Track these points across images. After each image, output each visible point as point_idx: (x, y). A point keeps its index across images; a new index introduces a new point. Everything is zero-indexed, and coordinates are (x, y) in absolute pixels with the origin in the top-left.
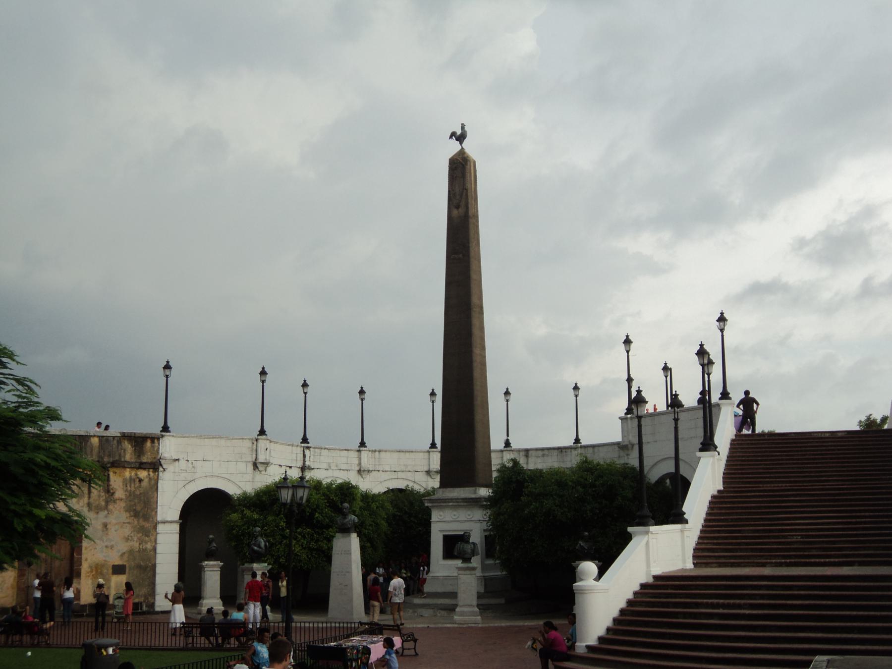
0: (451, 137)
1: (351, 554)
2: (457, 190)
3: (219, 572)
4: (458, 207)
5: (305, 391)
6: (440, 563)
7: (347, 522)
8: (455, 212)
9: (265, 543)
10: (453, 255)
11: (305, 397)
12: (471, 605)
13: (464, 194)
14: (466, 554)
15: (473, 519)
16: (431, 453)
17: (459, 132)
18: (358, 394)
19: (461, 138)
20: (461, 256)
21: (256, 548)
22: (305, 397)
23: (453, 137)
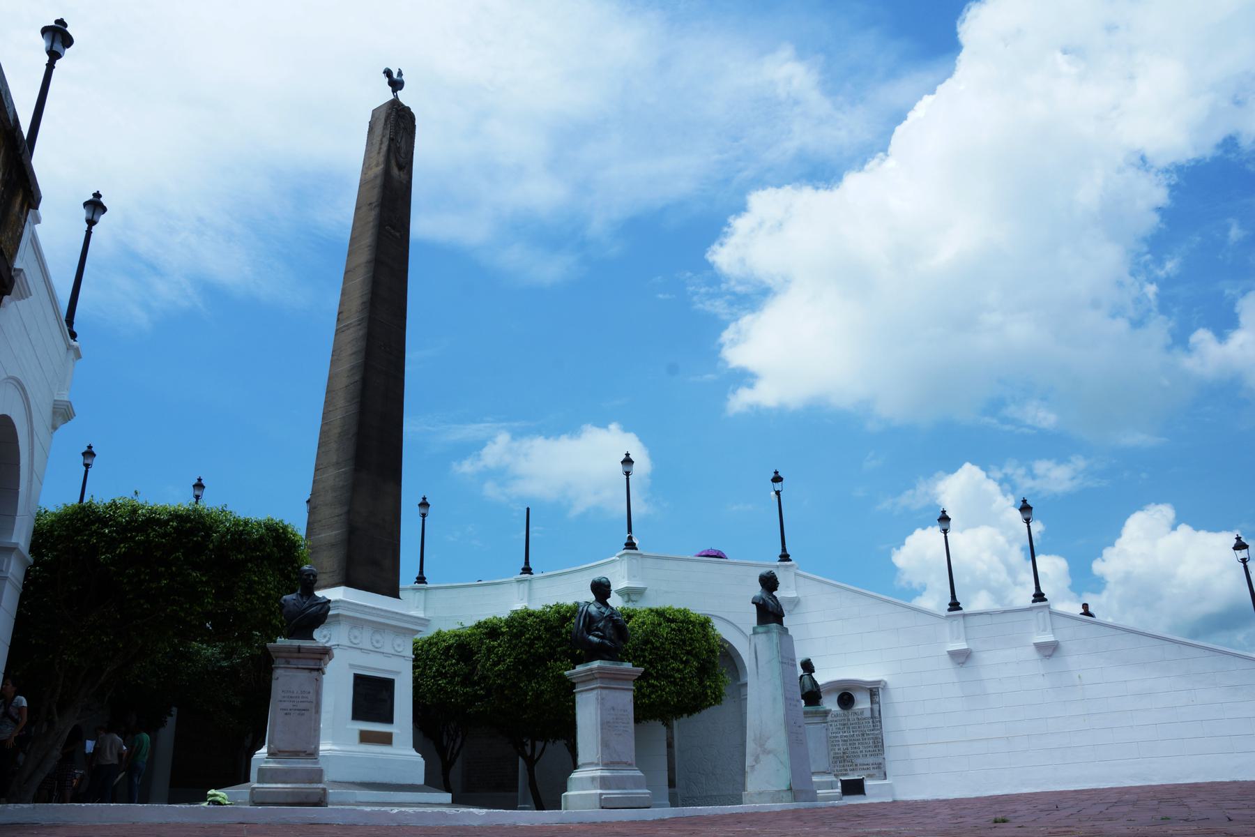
4: (400, 168)
6: (348, 727)
8: (395, 171)
19: (396, 84)
20: (398, 234)
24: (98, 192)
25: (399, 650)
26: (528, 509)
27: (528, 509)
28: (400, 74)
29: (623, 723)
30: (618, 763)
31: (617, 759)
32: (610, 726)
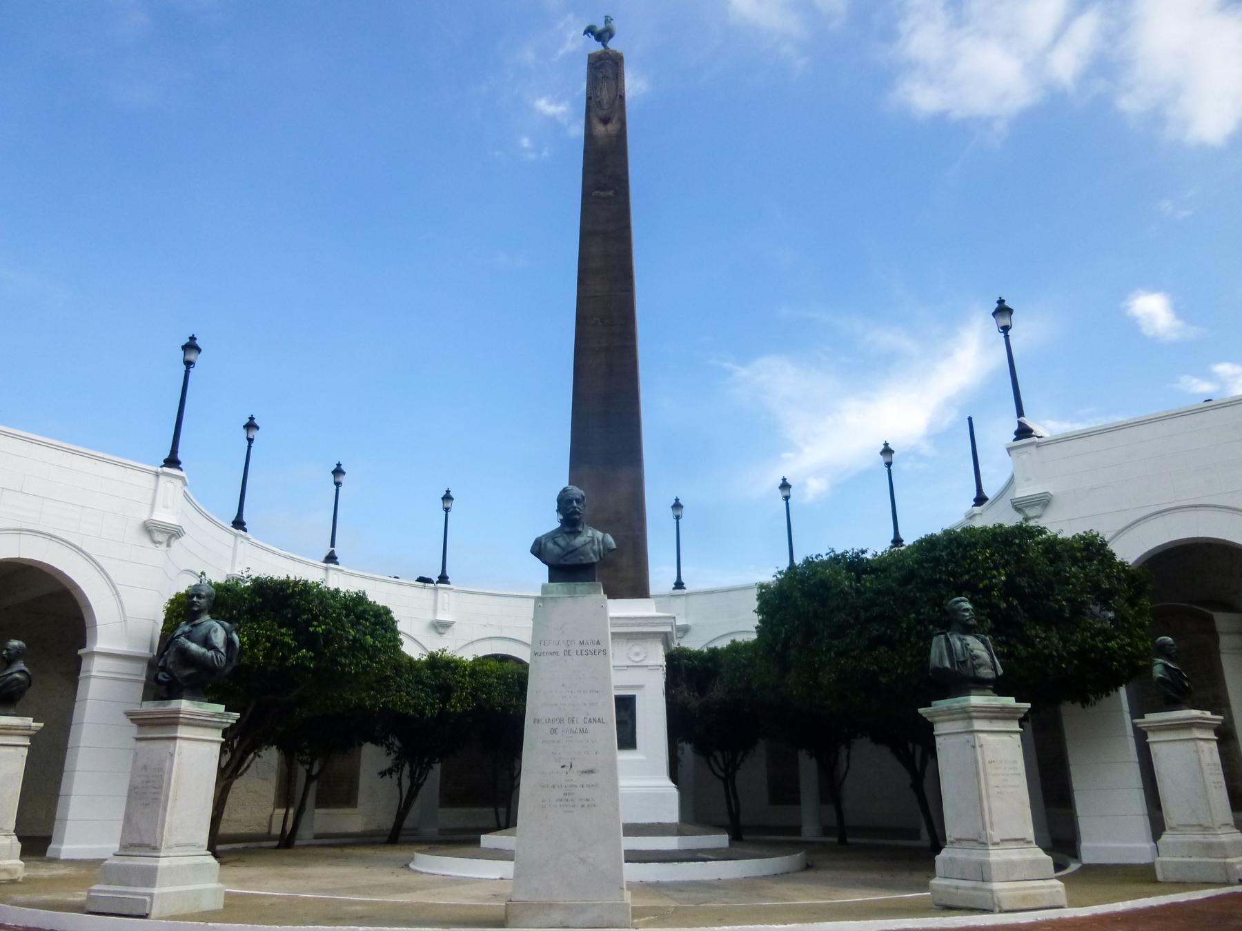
0: (585, 33)
1: (605, 652)
2: (605, 95)
3: (25, 751)
4: (605, 121)
5: (251, 436)
7: (586, 544)
8: (600, 129)
9: (228, 633)
10: (597, 192)
11: (249, 447)
12: (1023, 840)
13: (617, 102)
14: (980, 665)
15: (645, 663)
16: (440, 592)
17: (600, 26)
18: (333, 476)
19: (602, 36)
20: (611, 193)
21: (194, 647)
22: (249, 447)
23: (590, 34)
24: (193, 335)
25: (637, 659)
26: (970, 419)
27: (970, 419)
28: (608, 20)
29: (154, 787)
30: (140, 846)
31: (137, 841)
32: (136, 793)
